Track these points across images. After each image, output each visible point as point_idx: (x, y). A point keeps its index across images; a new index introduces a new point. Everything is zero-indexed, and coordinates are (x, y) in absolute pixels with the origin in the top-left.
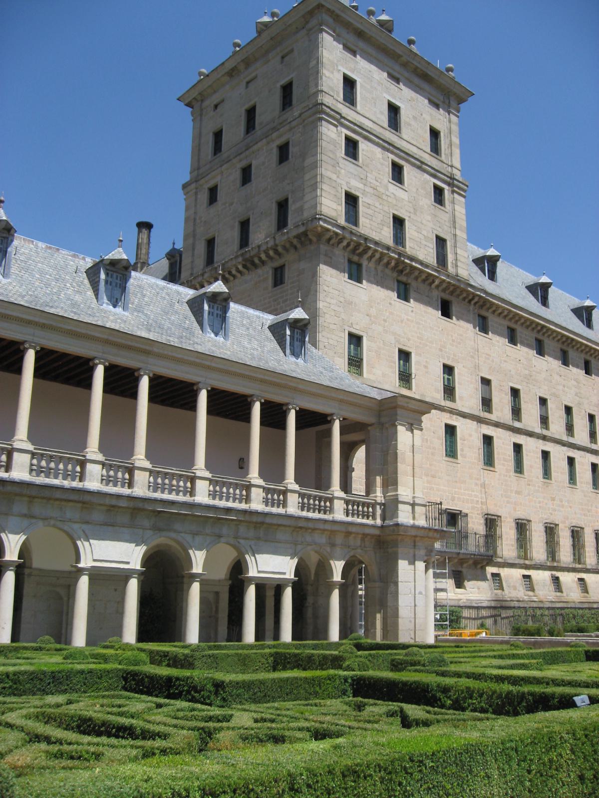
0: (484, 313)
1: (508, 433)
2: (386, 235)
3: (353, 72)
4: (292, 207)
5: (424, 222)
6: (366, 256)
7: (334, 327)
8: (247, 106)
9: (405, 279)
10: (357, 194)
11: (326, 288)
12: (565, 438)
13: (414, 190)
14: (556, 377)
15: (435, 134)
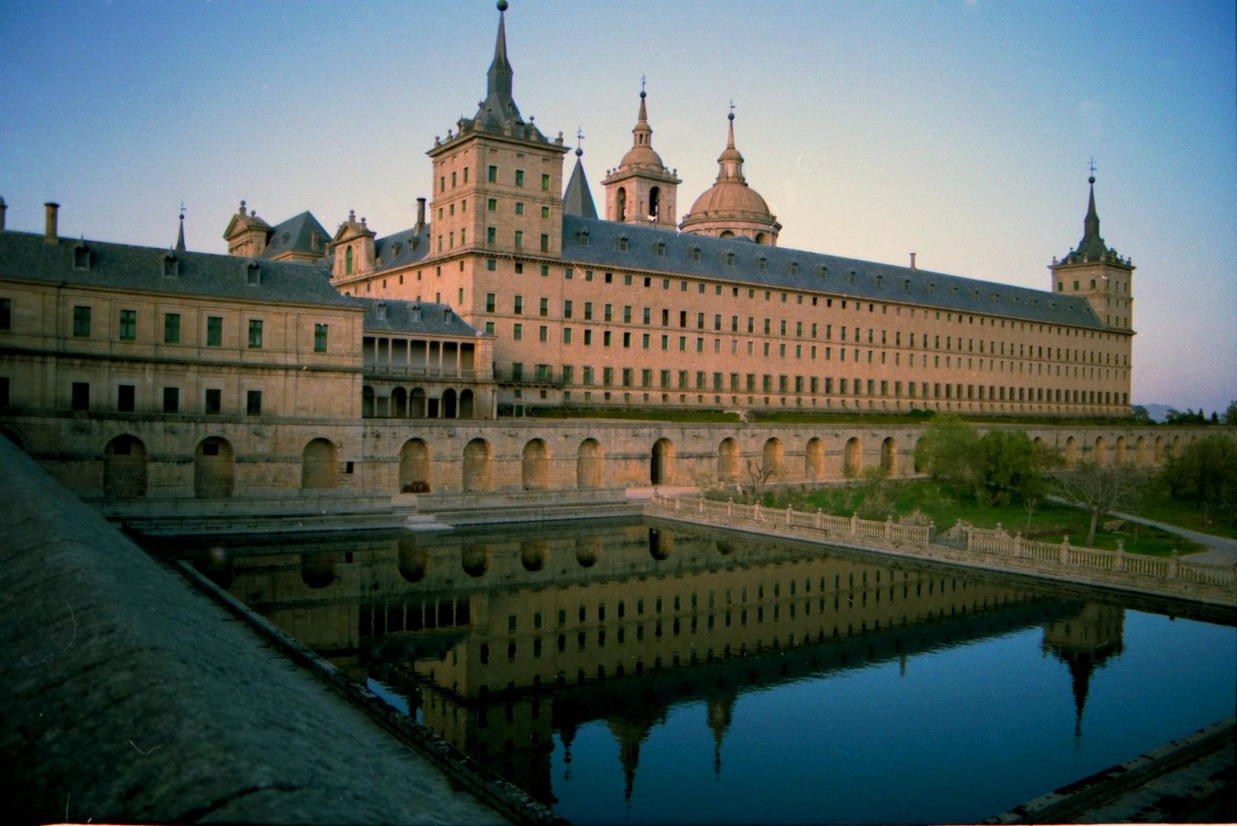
2: (512, 242)
15: (545, 177)
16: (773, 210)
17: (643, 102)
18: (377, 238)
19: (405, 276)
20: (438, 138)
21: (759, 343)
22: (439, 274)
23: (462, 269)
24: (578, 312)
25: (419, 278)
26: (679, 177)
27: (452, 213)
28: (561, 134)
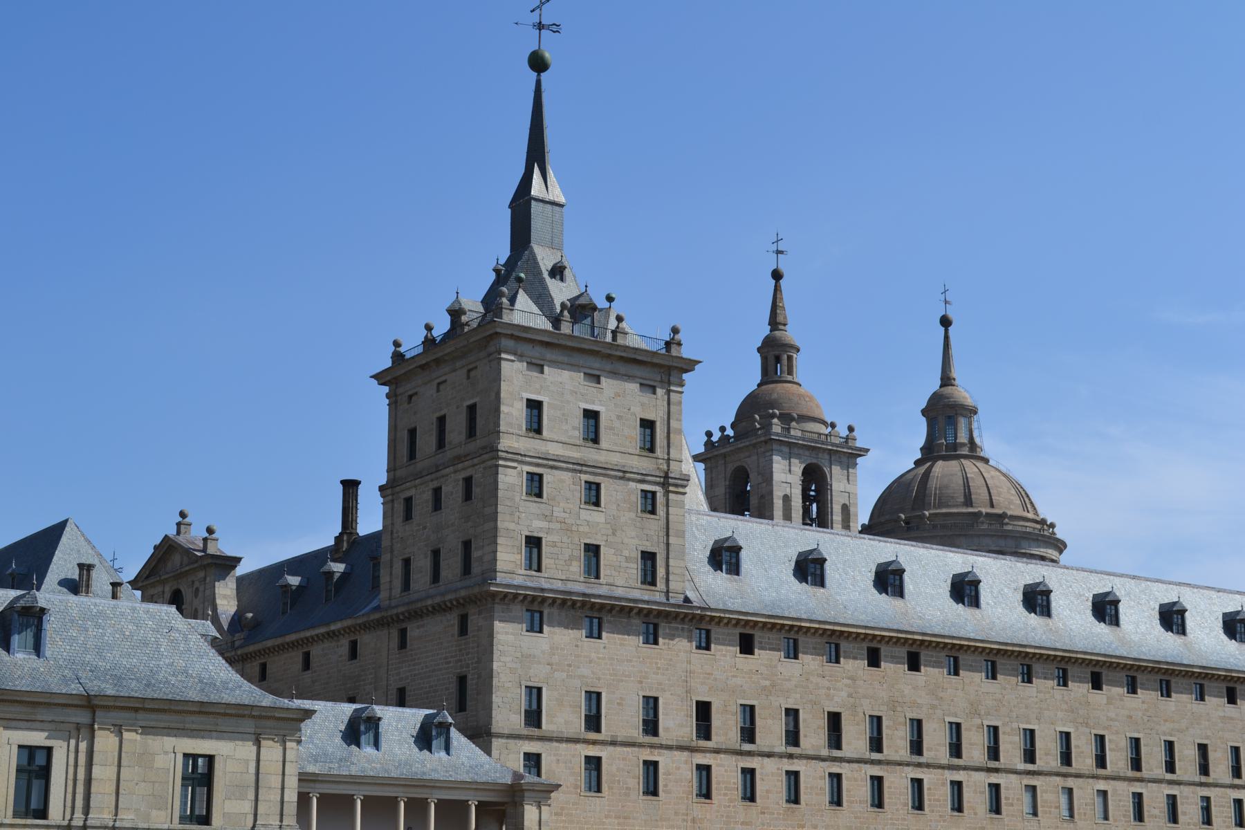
0: (703, 626)
1: (734, 758)
2: (577, 568)
3: (539, 393)
4: (475, 554)
5: (626, 540)
6: (546, 604)
7: (510, 685)
8: (438, 414)
9: (595, 615)
10: (540, 535)
11: (501, 647)
12: (825, 752)
13: (614, 507)
14: (814, 679)
16: (1046, 512)
17: (777, 289)
18: (240, 570)
19: (316, 651)
20: (397, 344)
21: (1121, 794)
22: (403, 644)
23: (463, 630)
24: (726, 727)
25: (353, 654)
26: (858, 444)
27: (437, 504)
28: (675, 331)
